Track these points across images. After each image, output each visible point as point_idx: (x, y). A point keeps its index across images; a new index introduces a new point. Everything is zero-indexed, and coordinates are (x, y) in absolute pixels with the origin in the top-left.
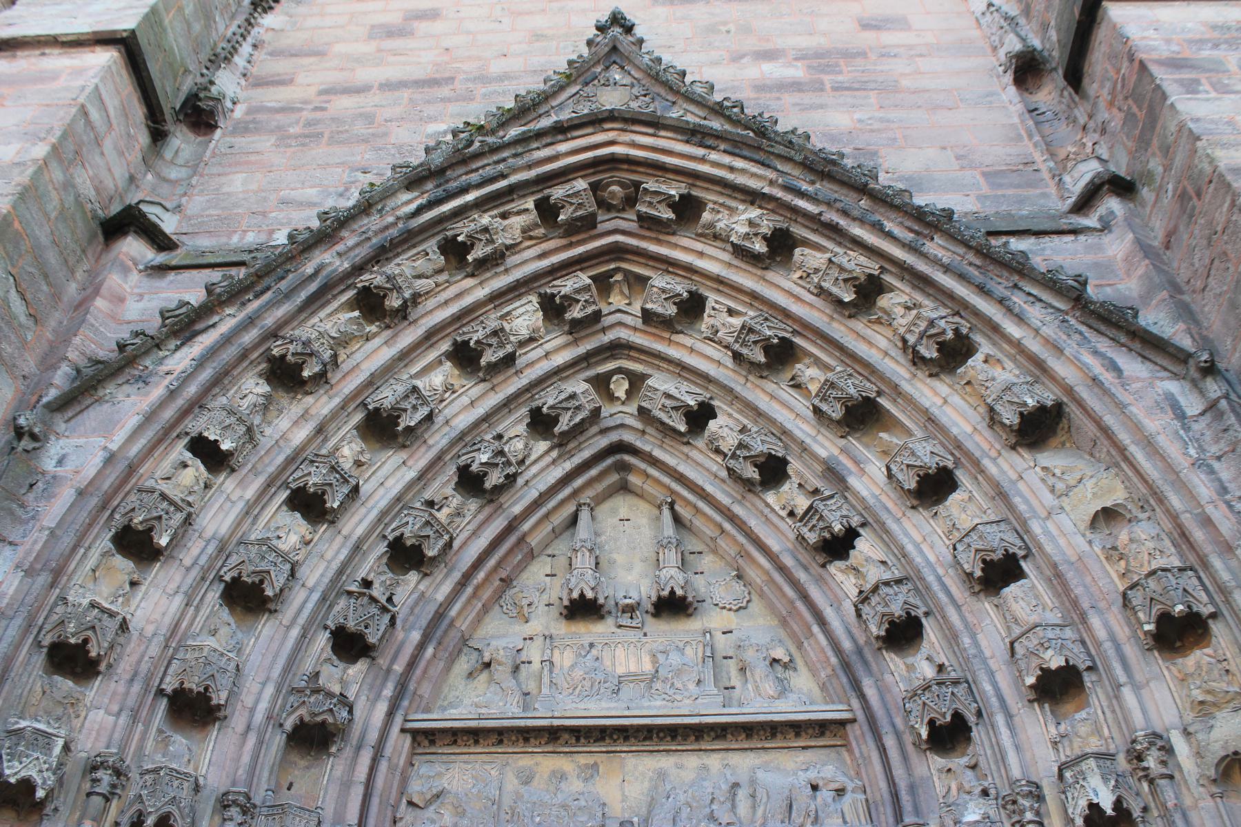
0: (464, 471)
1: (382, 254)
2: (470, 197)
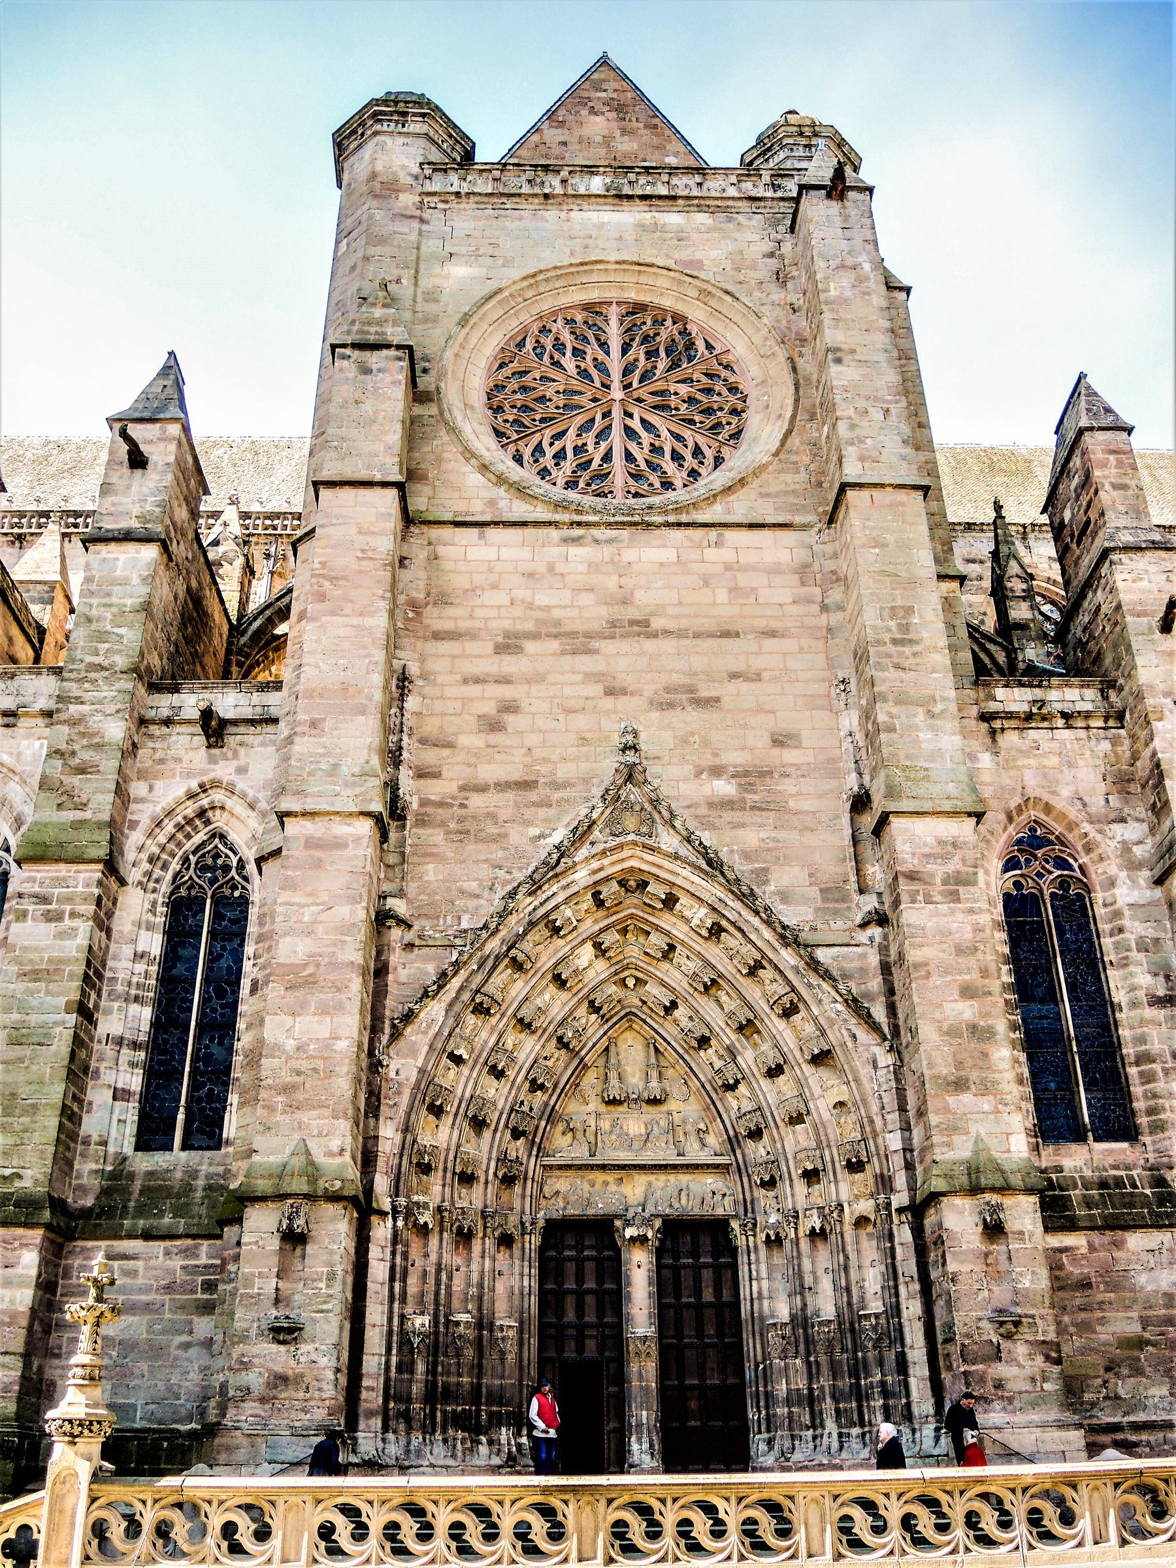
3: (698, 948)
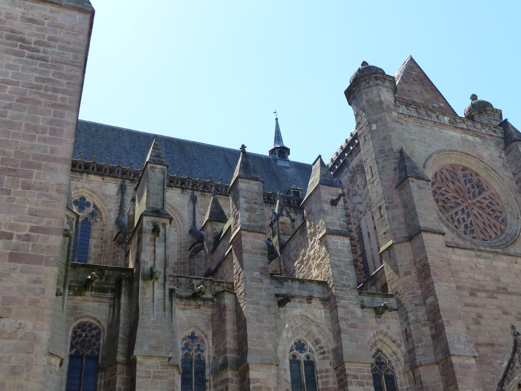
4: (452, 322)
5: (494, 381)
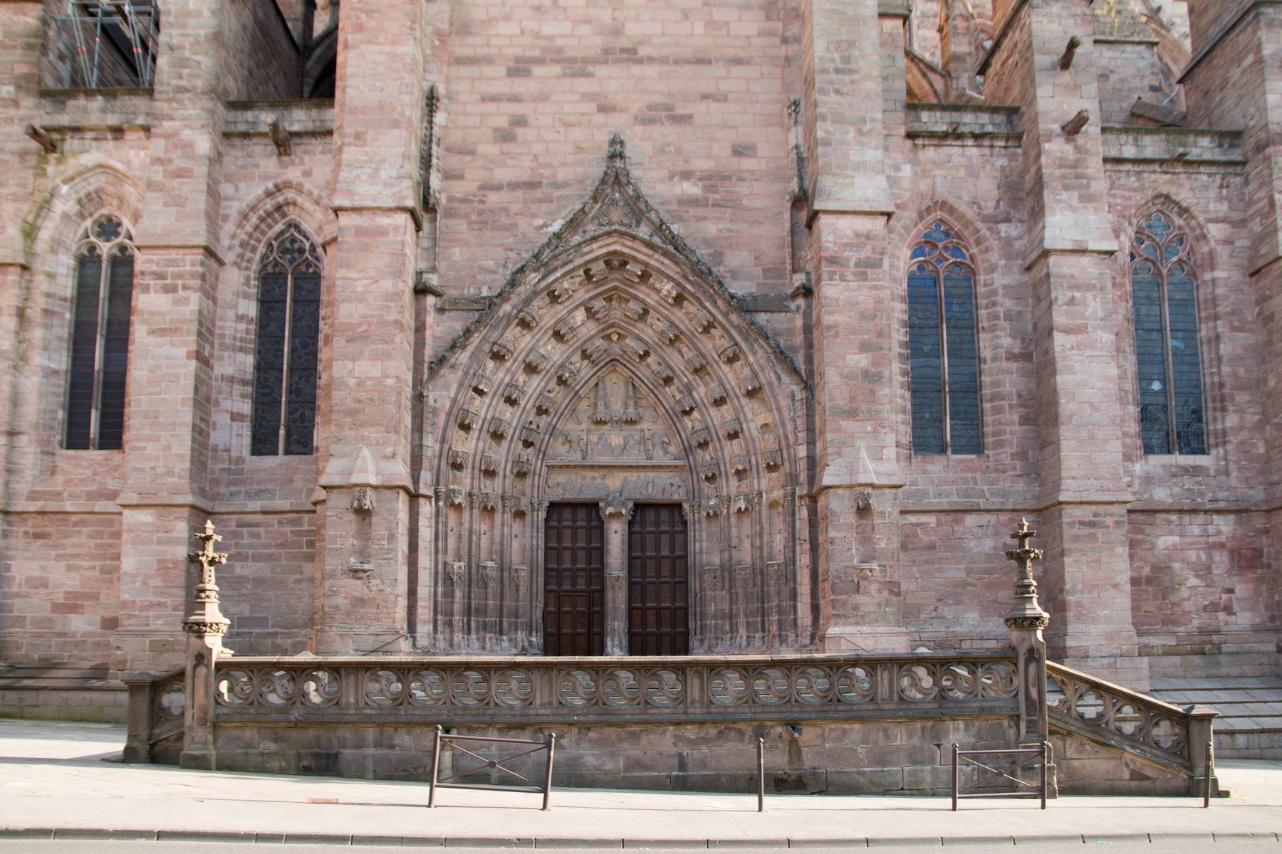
0: (560, 378)
1: (528, 302)
2: (558, 274)
3: (666, 312)
4: (369, 137)
5: (505, 266)
